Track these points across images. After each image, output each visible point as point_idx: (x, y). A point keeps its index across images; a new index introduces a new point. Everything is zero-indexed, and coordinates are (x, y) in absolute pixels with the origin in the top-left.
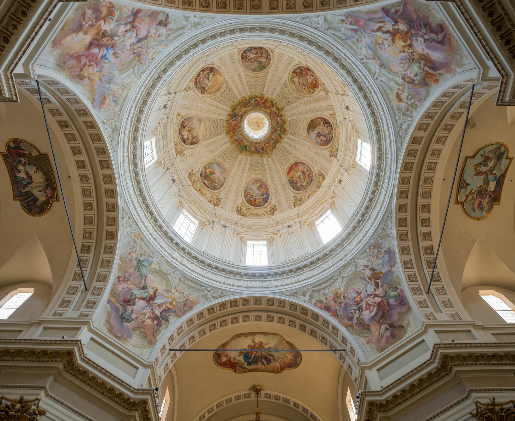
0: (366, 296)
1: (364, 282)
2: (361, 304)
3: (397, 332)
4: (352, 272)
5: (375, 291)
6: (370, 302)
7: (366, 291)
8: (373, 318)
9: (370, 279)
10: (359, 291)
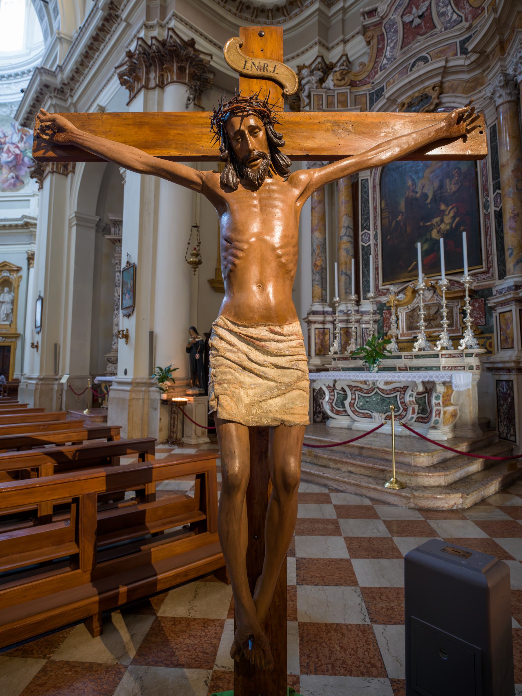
0: (10, 142)
1: (13, 129)
2: (3, 146)
3: (18, 184)
4: (5, 114)
5: (19, 143)
6: (11, 149)
7: (12, 138)
8: (8, 163)
9: (19, 131)
10: (6, 135)
